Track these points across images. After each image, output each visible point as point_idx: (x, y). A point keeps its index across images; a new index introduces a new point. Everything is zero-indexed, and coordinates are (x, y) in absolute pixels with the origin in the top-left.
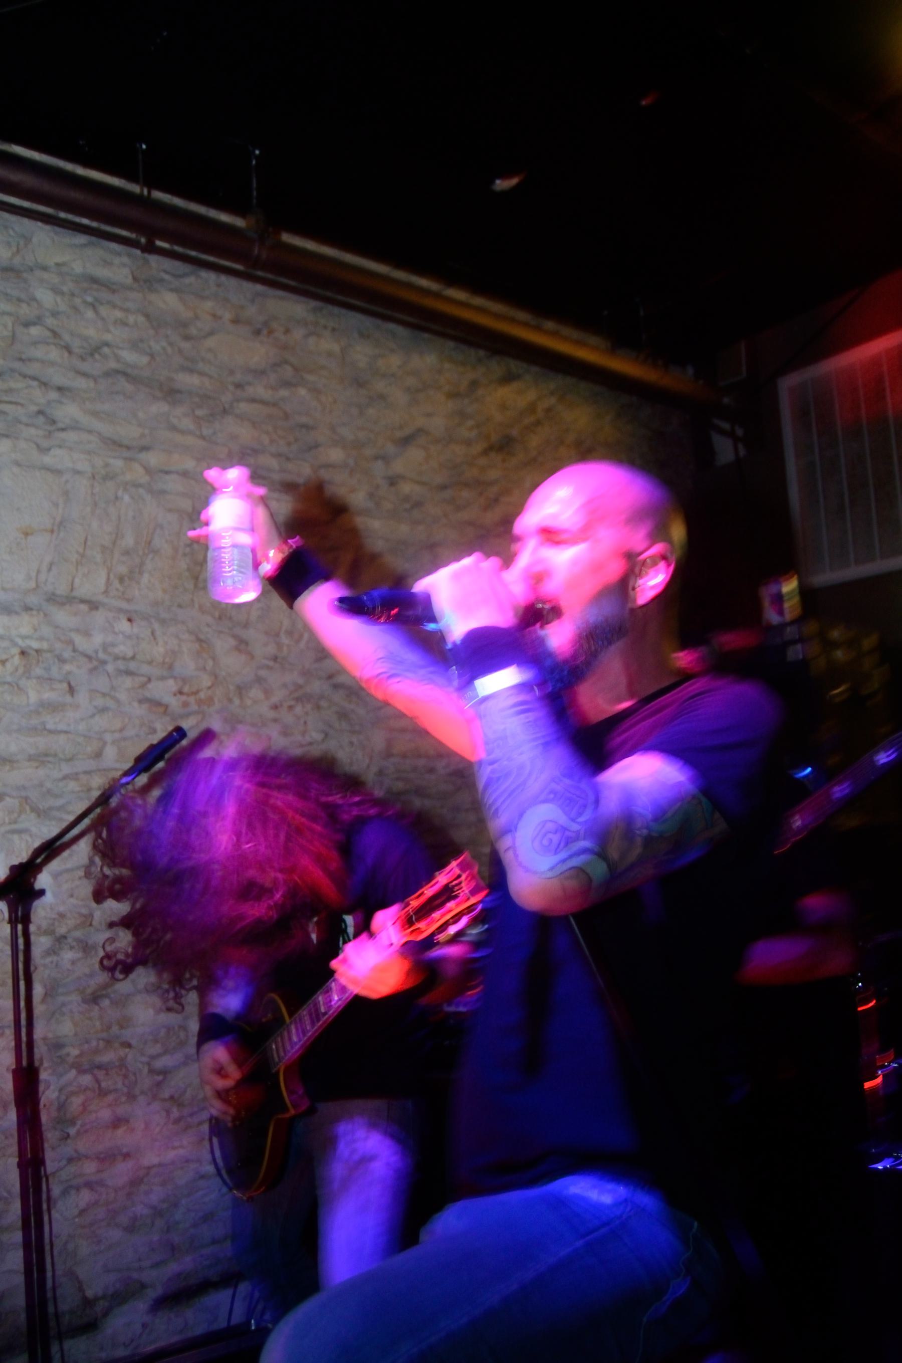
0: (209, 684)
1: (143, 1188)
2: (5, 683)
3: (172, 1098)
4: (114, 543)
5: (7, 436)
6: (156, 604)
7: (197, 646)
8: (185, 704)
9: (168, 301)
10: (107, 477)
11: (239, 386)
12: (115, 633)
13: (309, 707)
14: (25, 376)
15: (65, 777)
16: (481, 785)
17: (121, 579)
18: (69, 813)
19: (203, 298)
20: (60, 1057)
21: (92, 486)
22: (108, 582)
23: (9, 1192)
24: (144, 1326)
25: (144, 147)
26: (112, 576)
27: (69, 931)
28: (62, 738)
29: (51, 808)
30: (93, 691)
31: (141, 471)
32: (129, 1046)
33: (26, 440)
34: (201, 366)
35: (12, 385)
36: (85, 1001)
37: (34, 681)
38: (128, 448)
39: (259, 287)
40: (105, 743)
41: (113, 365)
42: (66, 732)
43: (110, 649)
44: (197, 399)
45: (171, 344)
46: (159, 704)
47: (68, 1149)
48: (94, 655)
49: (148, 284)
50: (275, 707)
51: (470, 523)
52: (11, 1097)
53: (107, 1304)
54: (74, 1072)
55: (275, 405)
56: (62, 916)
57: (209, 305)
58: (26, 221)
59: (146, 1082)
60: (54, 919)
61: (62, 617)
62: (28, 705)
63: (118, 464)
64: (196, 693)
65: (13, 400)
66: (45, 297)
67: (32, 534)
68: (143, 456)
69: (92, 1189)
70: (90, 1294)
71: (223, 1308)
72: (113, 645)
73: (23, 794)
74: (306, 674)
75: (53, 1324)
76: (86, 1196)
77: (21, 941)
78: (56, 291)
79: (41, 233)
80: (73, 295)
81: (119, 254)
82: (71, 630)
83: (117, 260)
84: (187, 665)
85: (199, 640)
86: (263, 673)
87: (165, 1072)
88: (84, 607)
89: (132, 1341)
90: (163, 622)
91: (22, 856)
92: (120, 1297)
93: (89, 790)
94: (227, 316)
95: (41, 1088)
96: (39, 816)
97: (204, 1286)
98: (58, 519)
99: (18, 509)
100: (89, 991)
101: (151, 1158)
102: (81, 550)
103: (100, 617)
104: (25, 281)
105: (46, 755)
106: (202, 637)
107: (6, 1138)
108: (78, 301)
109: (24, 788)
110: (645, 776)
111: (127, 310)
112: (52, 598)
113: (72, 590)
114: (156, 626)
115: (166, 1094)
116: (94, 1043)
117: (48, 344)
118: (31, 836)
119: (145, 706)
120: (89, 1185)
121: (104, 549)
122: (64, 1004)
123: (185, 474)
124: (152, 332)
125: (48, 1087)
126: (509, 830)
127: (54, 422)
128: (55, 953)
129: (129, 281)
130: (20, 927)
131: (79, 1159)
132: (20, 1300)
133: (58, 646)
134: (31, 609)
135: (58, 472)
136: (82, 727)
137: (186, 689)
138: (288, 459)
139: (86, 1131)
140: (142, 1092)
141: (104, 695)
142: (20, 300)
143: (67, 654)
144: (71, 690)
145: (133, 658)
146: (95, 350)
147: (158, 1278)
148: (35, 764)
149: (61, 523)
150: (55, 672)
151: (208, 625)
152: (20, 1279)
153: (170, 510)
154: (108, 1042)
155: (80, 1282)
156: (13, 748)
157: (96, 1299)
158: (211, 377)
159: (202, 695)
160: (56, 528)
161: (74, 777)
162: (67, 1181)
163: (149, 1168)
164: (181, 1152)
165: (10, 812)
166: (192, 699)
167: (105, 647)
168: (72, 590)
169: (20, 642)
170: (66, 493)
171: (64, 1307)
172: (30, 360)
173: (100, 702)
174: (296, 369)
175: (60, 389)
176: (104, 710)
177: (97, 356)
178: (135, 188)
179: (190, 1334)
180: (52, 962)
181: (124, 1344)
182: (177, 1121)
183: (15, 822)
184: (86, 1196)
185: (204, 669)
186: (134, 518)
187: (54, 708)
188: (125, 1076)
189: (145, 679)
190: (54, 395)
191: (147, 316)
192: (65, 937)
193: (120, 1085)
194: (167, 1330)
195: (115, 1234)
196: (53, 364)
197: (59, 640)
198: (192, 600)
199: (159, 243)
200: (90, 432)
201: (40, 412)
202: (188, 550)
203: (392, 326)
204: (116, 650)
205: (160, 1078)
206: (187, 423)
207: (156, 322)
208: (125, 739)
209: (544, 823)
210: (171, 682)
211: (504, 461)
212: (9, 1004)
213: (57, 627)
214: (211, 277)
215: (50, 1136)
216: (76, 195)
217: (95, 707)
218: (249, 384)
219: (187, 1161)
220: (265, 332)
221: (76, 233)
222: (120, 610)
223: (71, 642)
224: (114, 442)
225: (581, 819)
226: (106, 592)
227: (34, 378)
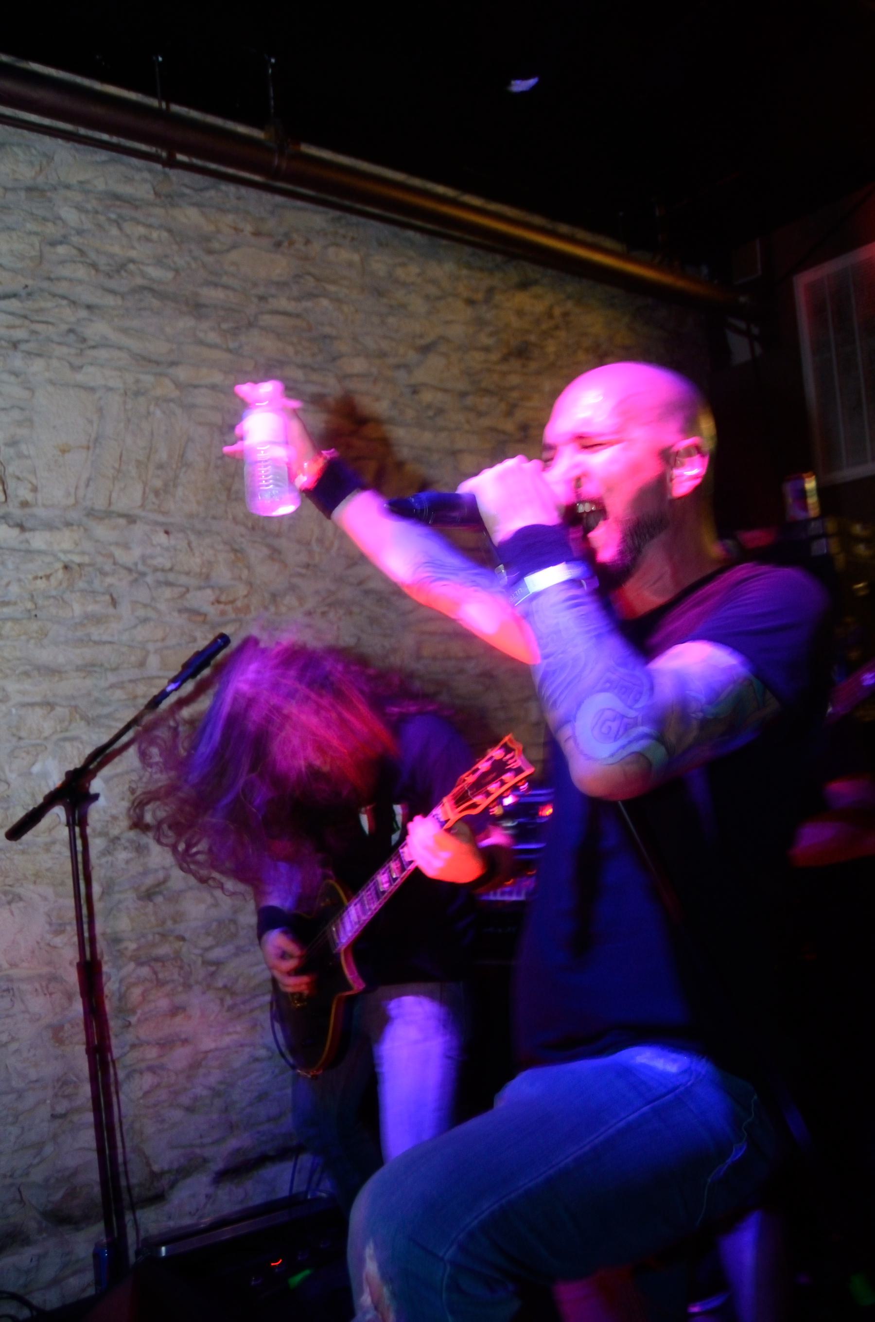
0: (245, 593)
1: (202, 1071)
2: (50, 597)
3: (225, 987)
4: (148, 458)
5: (39, 355)
6: (191, 516)
7: (232, 556)
8: (223, 613)
9: (189, 216)
10: (137, 394)
11: (262, 298)
12: (153, 545)
13: (341, 612)
14: (54, 295)
15: (112, 686)
16: (537, 679)
17: (157, 493)
18: (116, 720)
19: (222, 210)
20: (119, 951)
21: (125, 403)
22: (144, 497)
23: (77, 1077)
24: (208, 1196)
25: (160, 59)
26: (147, 490)
27: (122, 833)
28: (107, 648)
29: (99, 717)
30: (135, 603)
31: (171, 386)
32: (183, 939)
33: (60, 359)
34: (225, 279)
35: (43, 304)
36: (140, 898)
37: (78, 594)
38: (158, 363)
39: (279, 199)
40: (148, 652)
41: (139, 281)
42: (111, 643)
43: (149, 562)
44: (222, 313)
45: (195, 259)
46: (197, 613)
47: (130, 1037)
48: (133, 567)
49: (170, 199)
50: (309, 614)
51: (493, 429)
52: (77, 989)
53: (172, 1177)
54: (132, 965)
55: (298, 316)
56: (115, 818)
57: (230, 218)
58: (47, 139)
59: (200, 973)
60: (108, 821)
61: (101, 531)
62: (73, 617)
63: (148, 379)
64: (232, 602)
65: (44, 319)
67: (69, 451)
68: (171, 371)
69: (154, 1073)
70: (156, 1168)
71: (281, 1179)
72: (152, 557)
73: (73, 703)
74: (340, 580)
75: (125, 1196)
76: (148, 1080)
77: (79, 842)
78: (80, 208)
79: (62, 150)
80: (97, 212)
81: (139, 170)
82: (111, 544)
83: (138, 177)
84: (223, 574)
85: (235, 551)
86: (295, 580)
87: (218, 963)
88: (122, 521)
89: (197, 1210)
90: (199, 533)
91: (76, 763)
92: (183, 1172)
93: (135, 697)
94: (248, 228)
95: (104, 978)
96: (89, 724)
97: (262, 1160)
98: (93, 436)
99: (54, 427)
100: (143, 889)
101: (207, 1044)
102: (117, 465)
103: (139, 529)
104: (50, 200)
105: (93, 665)
106: (236, 547)
107: (73, 1027)
108: (102, 218)
109: (73, 698)
110: (696, 663)
111: (150, 226)
112: (91, 513)
113: (110, 504)
114: (192, 538)
115: (220, 984)
116: (150, 937)
117: (74, 262)
118: (82, 742)
119: (185, 616)
120: (151, 1069)
121: (139, 463)
122: (120, 902)
123: (213, 387)
124: (175, 247)
125: (110, 979)
126: (568, 720)
127: (84, 340)
128: (109, 853)
129: (151, 196)
130: (77, 829)
131: (141, 1045)
132: (94, 1175)
133: (99, 559)
134: (72, 525)
135: (92, 390)
136: (125, 637)
137: (223, 598)
138: (313, 370)
139: (146, 1019)
140: (197, 982)
141: (145, 606)
142: (45, 219)
143: (108, 568)
144: (114, 603)
145: (171, 570)
146: (121, 267)
147: (219, 1155)
148: (83, 674)
149: (96, 440)
150: (97, 585)
151: (242, 536)
152: (94, 1156)
153: (200, 424)
154: (164, 936)
155: (146, 1158)
156: (61, 659)
157: (162, 1173)
158: (234, 290)
159: (239, 604)
160: (91, 445)
161: (120, 685)
162: (131, 1065)
163: (207, 1052)
164: (235, 1037)
165: (62, 721)
166: (229, 608)
167: (144, 558)
168: (110, 504)
169: (62, 556)
170: (100, 410)
171: (134, 1181)
172: (59, 279)
173: (141, 612)
174: (318, 279)
175: (89, 307)
176: (146, 620)
177: (123, 273)
178: (154, 102)
179: (251, 1204)
180: (107, 862)
181: (190, 1213)
182: (230, 1009)
183: (67, 730)
184: (148, 1080)
185: (240, 578)
186: (166, 432)
187: (98, 620)
188: (181, 968)
189: (184, 589)
190: (83, 313)
191: (170, 231)
192: (118, 838)
193: (176, 977)
194: (230, 1199)
195: (177, 1115)
196: (80, 282)
197: (100, 553)
198: (226, 512)
199: (180, 157)
200: (120, 348)
201: (71, 331)
202: (219, 462)
203: (410, 234)
205: (213, 968)
206: (213, 337)
207: (178, 236)
208: (167, 648)
209: (603, 711)
210: (209, 591)
211: (524, 366)
212: (71, 902)
213: (97, 541)
214: (231, 189)
215: (114, 1024)
216: (98, 111)
217: (137, 618)
218: (273, 296)
219: (242, 1045)
220: (286, 244)
221: (96, 149)
222: (157, 523)
223: (111, 556)
224: (144, 358)
225: (639, 706)
226: (143, 506)
227: (64, 297)
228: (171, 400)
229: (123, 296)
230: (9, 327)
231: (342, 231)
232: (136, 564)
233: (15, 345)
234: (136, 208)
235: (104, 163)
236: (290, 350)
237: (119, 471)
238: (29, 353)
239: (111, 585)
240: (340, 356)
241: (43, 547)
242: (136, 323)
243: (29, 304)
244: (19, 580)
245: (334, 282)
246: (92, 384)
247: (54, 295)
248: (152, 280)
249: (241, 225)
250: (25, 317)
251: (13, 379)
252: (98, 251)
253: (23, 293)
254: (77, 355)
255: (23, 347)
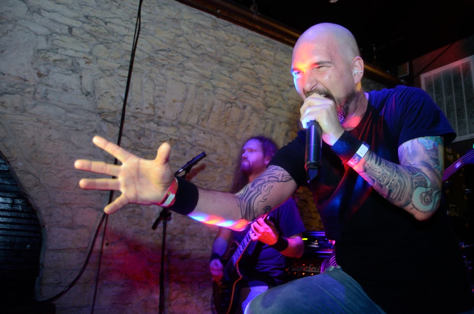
3: (206, 297)
5: (171, 70)
6: (212, 129)
9: (221, 34)
10: (200, 87)
11: (242, 62)
17: (202, 120)
22: (198, 121)
31: (211, 86)
34: (230, 55)
38: (207, 78)
49: (216, 27)
56: (175, 228)
57: (234, 36)
61: (183, 130)
63: (204, 82)
66: (185, 28)
68: (211, 81)
78: (188, 26)
81: (208, 17)
82: (185, 134)
83: (207, 19)
85: (226, 143)
88: (190, 127)
90: (214, 135)
103: (195, 131)
108: (194, 30)
111: (208, 35)
112: (180, 123)
113: (187, 121)
114: (212, 136)
121: (198, 109)
123: (224, 88)
124: (216, 43)
127: (185, 67)
129: (210, 26)
135: (185, 83)
137: (220, 159)
138: (257, 88)
142: (177, 29)
143: (184, 142)
144: (184, 154)
145: (204, 146)
146: (199, 46)
151: (228, 139)
167: (196, 141)
168: (187, 121)
169: (169, 135)
170: (187, 90)
172: (179, 47)
174: (260, 59)
175: (187, 57)
177: (199, 48)
190: (185, 59)
191: (215, 37)
192: (175, 236)
196: (186, 49)
200: (196, 72)
201: (181, 64)
204: (199, 142)
210: (216, 155)
218: (245, 62)
220: (251, 46)
222: (201, 130)
223: (185, 138)
226: (197, 123)
227: (180, 53)
228: (209, 90)
229: (198, 55)
230: (162, 60)
231: (269, 45)
232: (193, 142)
233: (164, 65)
234: (206, 29)
235: (197, 14)
236: (249, 80)
237: (191, 111)
238: (168, 69)
239: (184, 148)
240: (265, 84)
241: (164, 132)
242: (201, 65)
243: (170, 54)
244: (155, 141)
245: (265, 61)
246: (186, 81)
247: (177, 52)
248: (208, 51)
249: (237, 39)
250: (167, 57)
251: (161, 76)
252: (192, 41)
253: (168, 50)
254: (182, 72)
255: (166, 66)
